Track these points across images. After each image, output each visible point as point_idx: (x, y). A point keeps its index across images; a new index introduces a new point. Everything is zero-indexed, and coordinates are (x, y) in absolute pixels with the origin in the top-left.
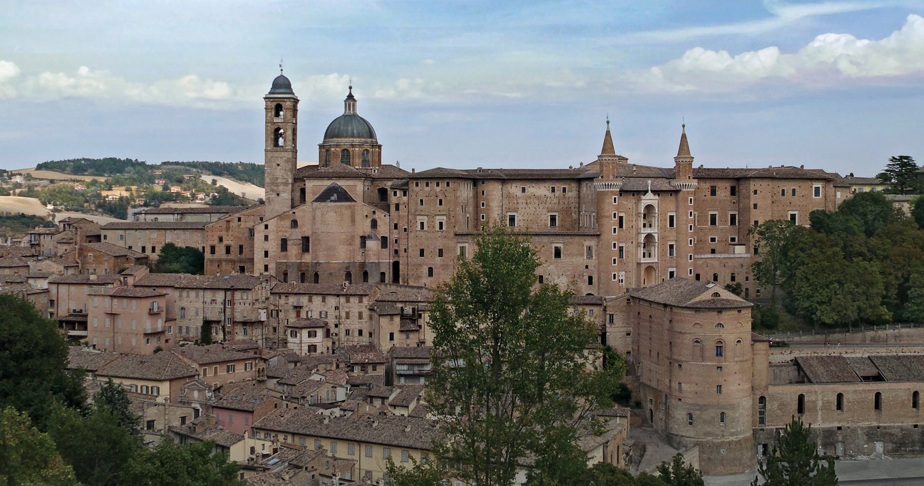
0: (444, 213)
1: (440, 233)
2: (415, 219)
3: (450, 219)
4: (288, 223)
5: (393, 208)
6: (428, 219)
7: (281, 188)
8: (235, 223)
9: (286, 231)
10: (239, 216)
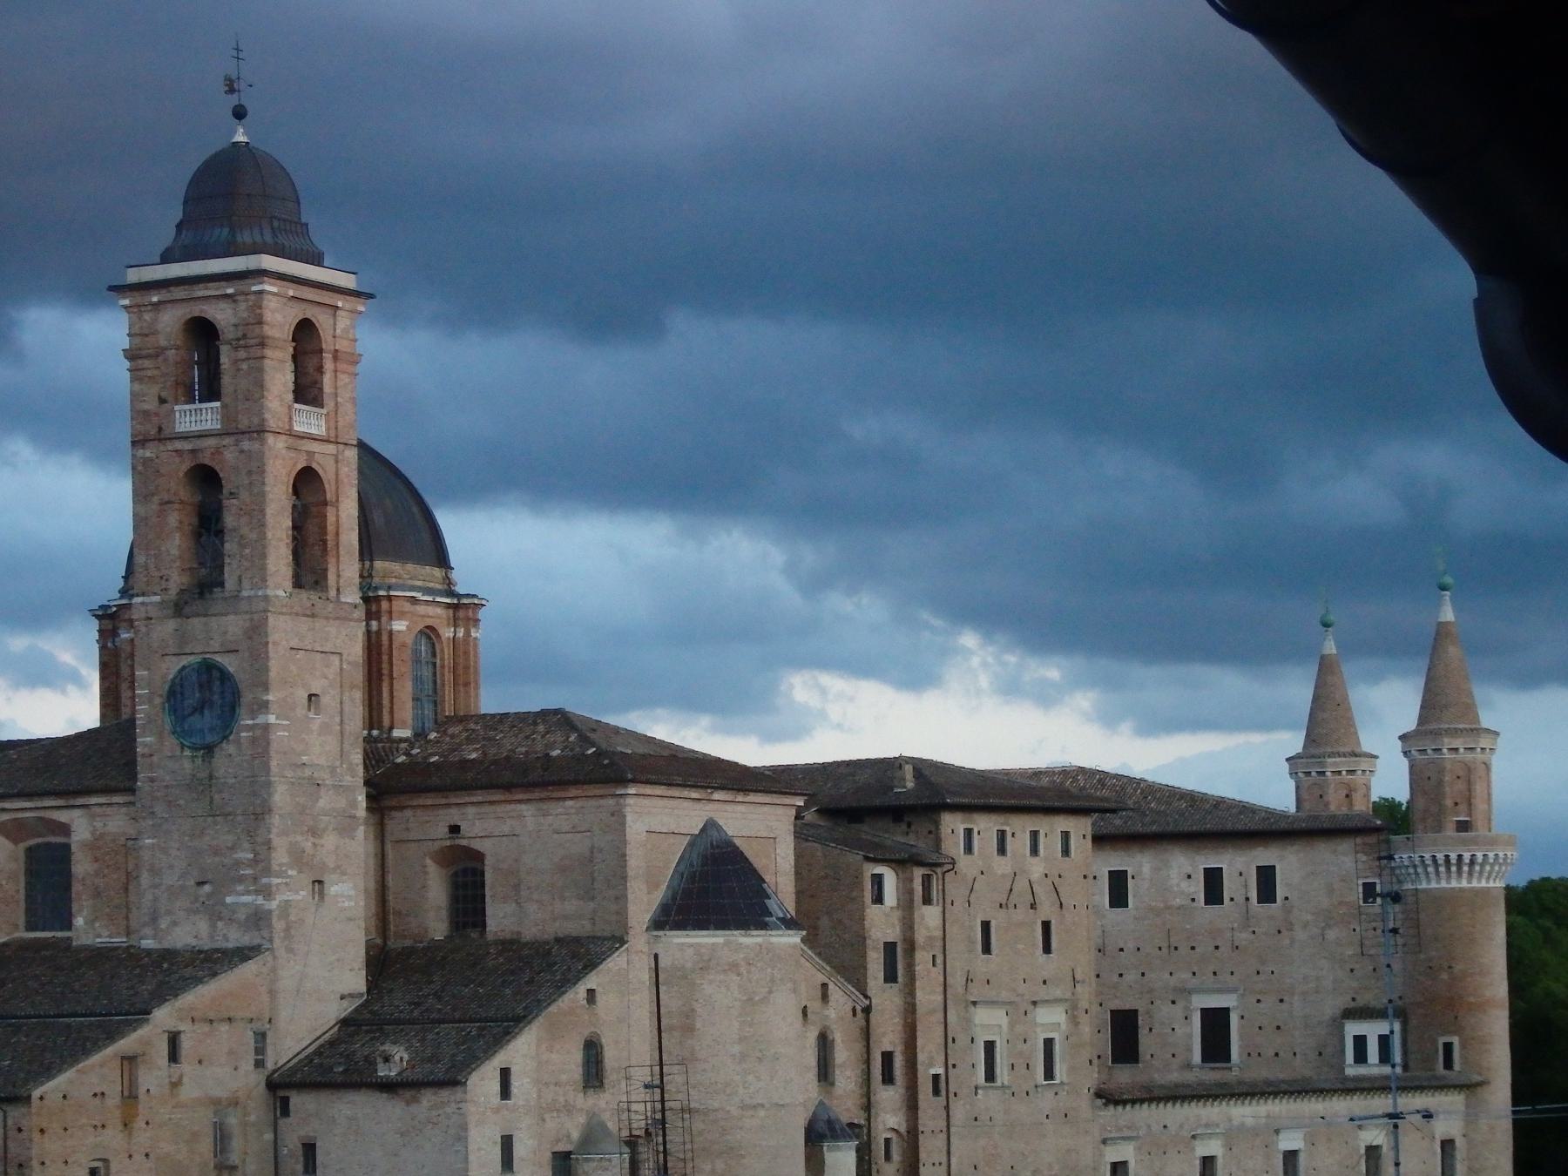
0: (1058, 993)
1: (1046, 1101)
2: (967, 1022)
3: (1077, 1024)
4: (572, 1060)
5: (875, 963)
6: (1012, 1025)
7: (330, 841)
8: (153, 1078)
9: (569, 1109)
10: (172, 1024)
